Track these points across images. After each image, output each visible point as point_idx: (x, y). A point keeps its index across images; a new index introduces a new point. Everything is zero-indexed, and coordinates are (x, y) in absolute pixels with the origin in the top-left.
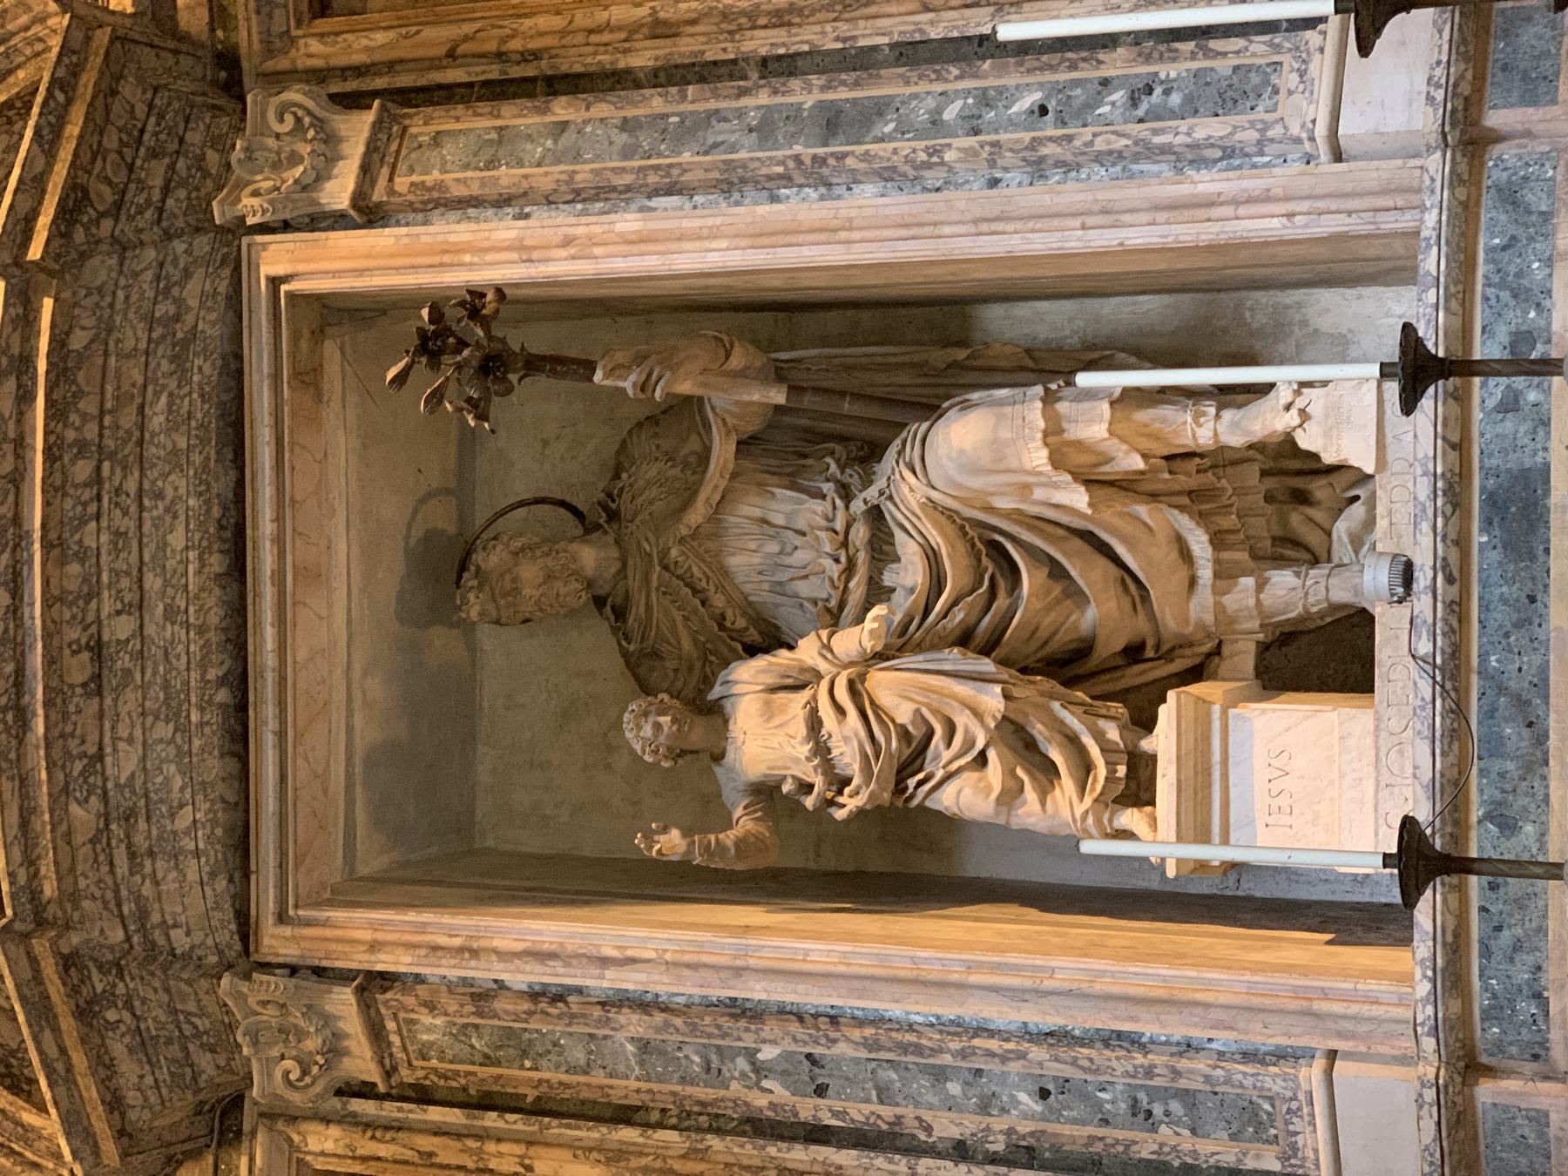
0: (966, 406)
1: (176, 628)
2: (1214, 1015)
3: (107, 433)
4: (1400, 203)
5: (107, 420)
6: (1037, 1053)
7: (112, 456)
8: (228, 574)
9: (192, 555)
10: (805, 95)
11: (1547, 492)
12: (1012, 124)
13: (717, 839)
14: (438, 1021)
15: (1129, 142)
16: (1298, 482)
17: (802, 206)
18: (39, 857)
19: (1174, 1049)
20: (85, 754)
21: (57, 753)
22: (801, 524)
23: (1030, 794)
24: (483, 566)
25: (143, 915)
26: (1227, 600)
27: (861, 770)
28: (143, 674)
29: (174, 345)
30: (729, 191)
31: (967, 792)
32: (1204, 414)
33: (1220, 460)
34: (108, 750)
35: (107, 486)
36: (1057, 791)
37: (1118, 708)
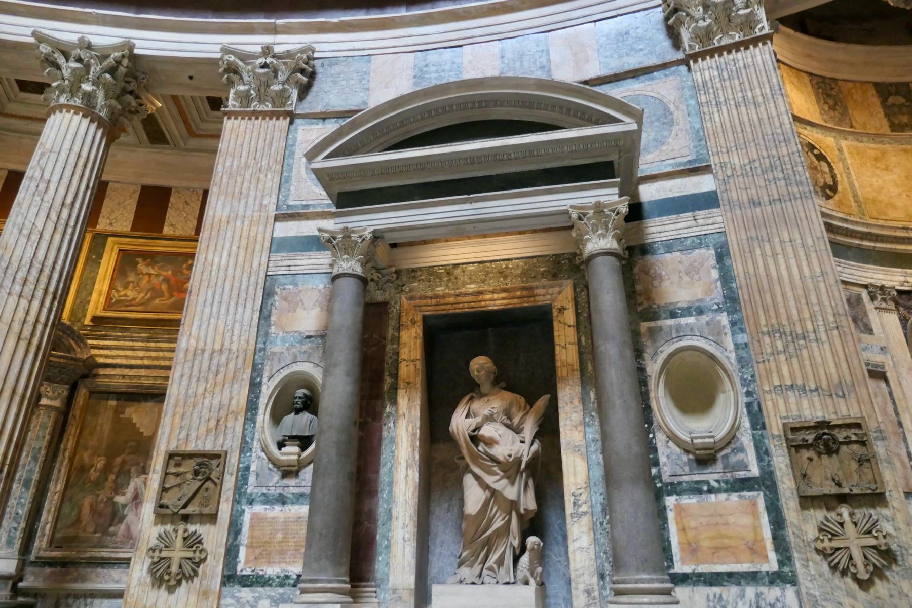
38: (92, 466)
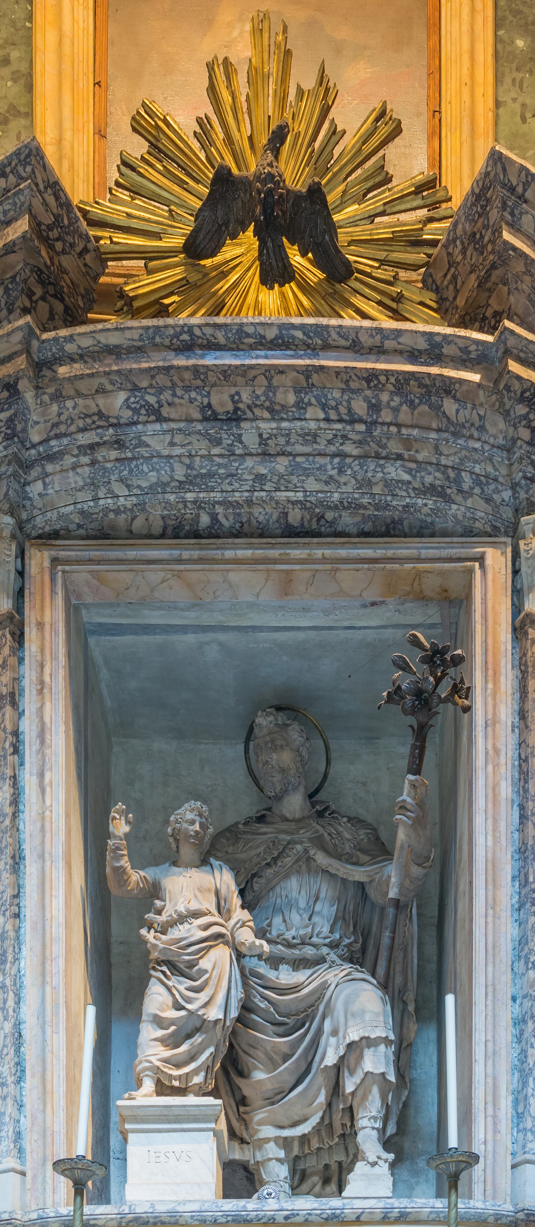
0: (384, 1003)
1: (251, 483)
2: (40, 1116)
3: (385, 428)
4: (488, 1192)
5: (393, 429)
7: (369, 431)
8: (288, 526)
9: (300, 495)
13: (123, 855)
15: (531, 1066)
18: (86, 362)
19: (18, 1098)
20: (161, 406)
21: (162, 380)
22: (315, 919)
23: (160, 1033)
24: (290, 728)
25: (51, 458)
26: (272, 1144)
27: (171, 939)
28: (218, 456)
29: (442, 487)
30: (520, 852)
31: (160, 998)
32: (375, 1122)
34: (165, 426)
35: (348, 427)
36: (163, 1048)
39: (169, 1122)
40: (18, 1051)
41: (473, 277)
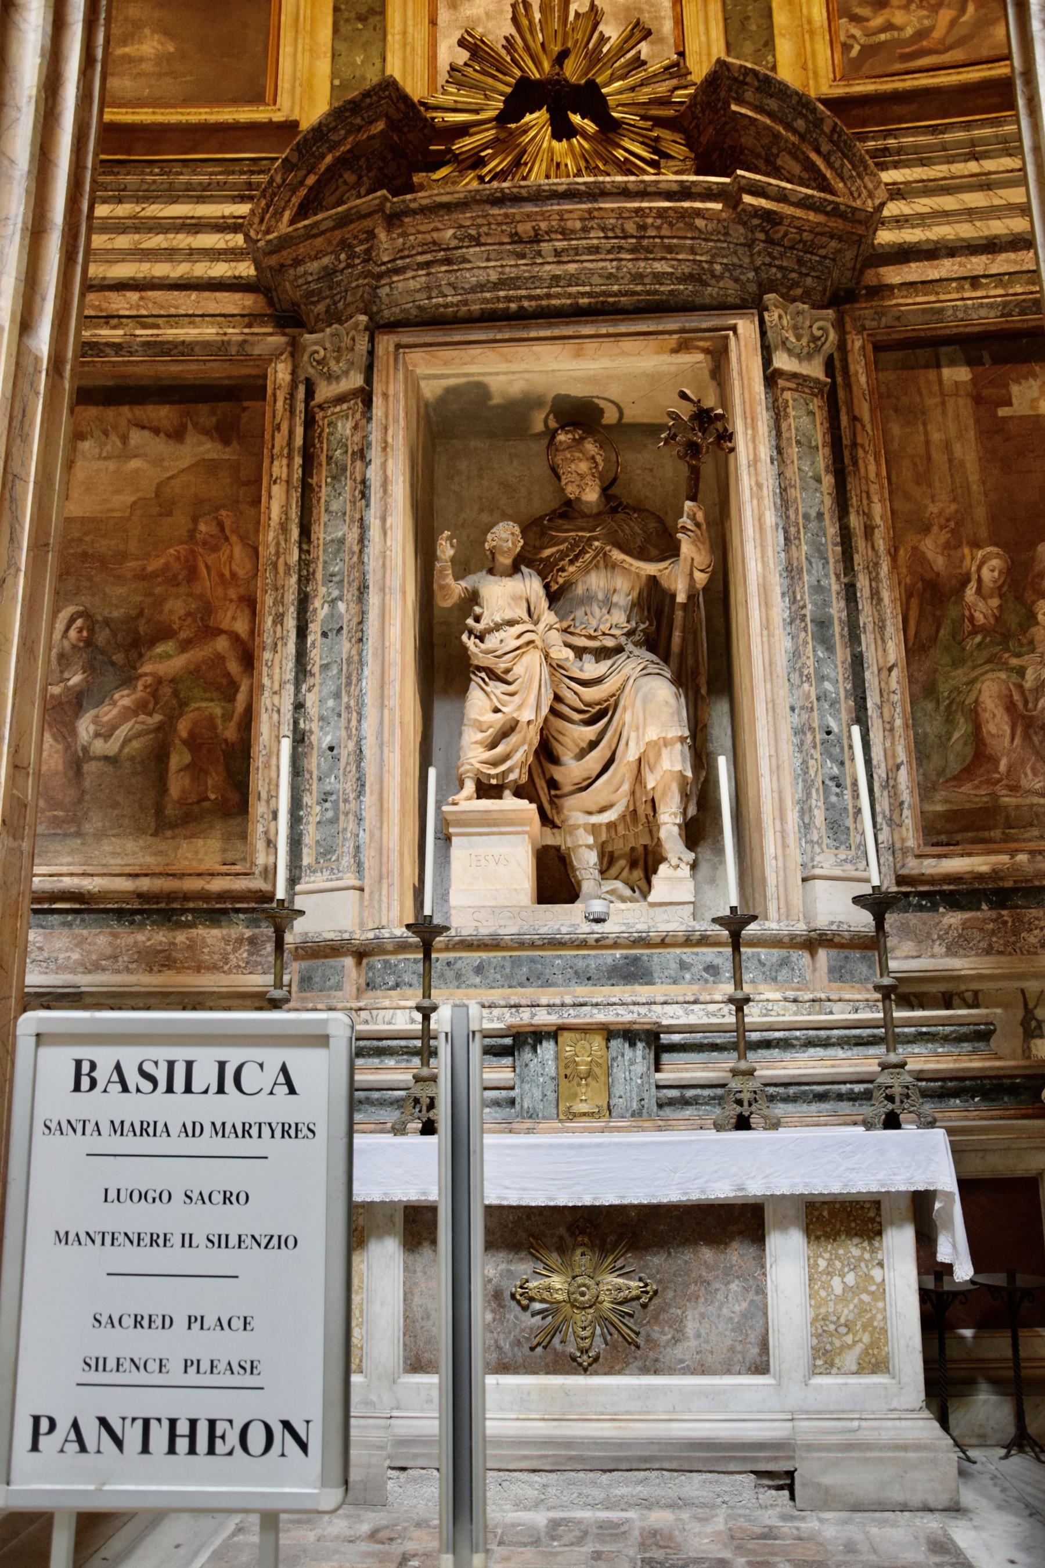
0: (677, 697)
2: (377, 833)
6: (351, 745)
10: (837, 609)
11: (641, 984)
12: (822, 717)
14: (348, 432)
16: (641, 863)
17: (780, 609)
23: (480, 736)
25: (397, 271)
26: (581, 831)
33: (652, 826)
37: (525, 778)
38: (966, 581)
39: (489, 825)
40: (358, 767)
41: (711, 127)
